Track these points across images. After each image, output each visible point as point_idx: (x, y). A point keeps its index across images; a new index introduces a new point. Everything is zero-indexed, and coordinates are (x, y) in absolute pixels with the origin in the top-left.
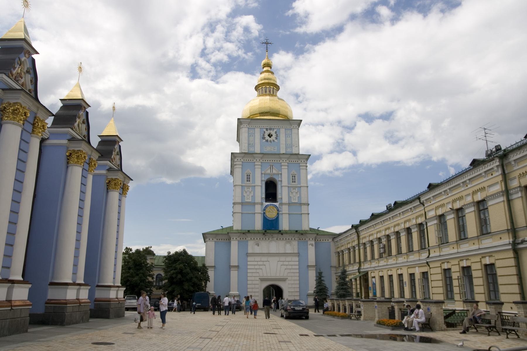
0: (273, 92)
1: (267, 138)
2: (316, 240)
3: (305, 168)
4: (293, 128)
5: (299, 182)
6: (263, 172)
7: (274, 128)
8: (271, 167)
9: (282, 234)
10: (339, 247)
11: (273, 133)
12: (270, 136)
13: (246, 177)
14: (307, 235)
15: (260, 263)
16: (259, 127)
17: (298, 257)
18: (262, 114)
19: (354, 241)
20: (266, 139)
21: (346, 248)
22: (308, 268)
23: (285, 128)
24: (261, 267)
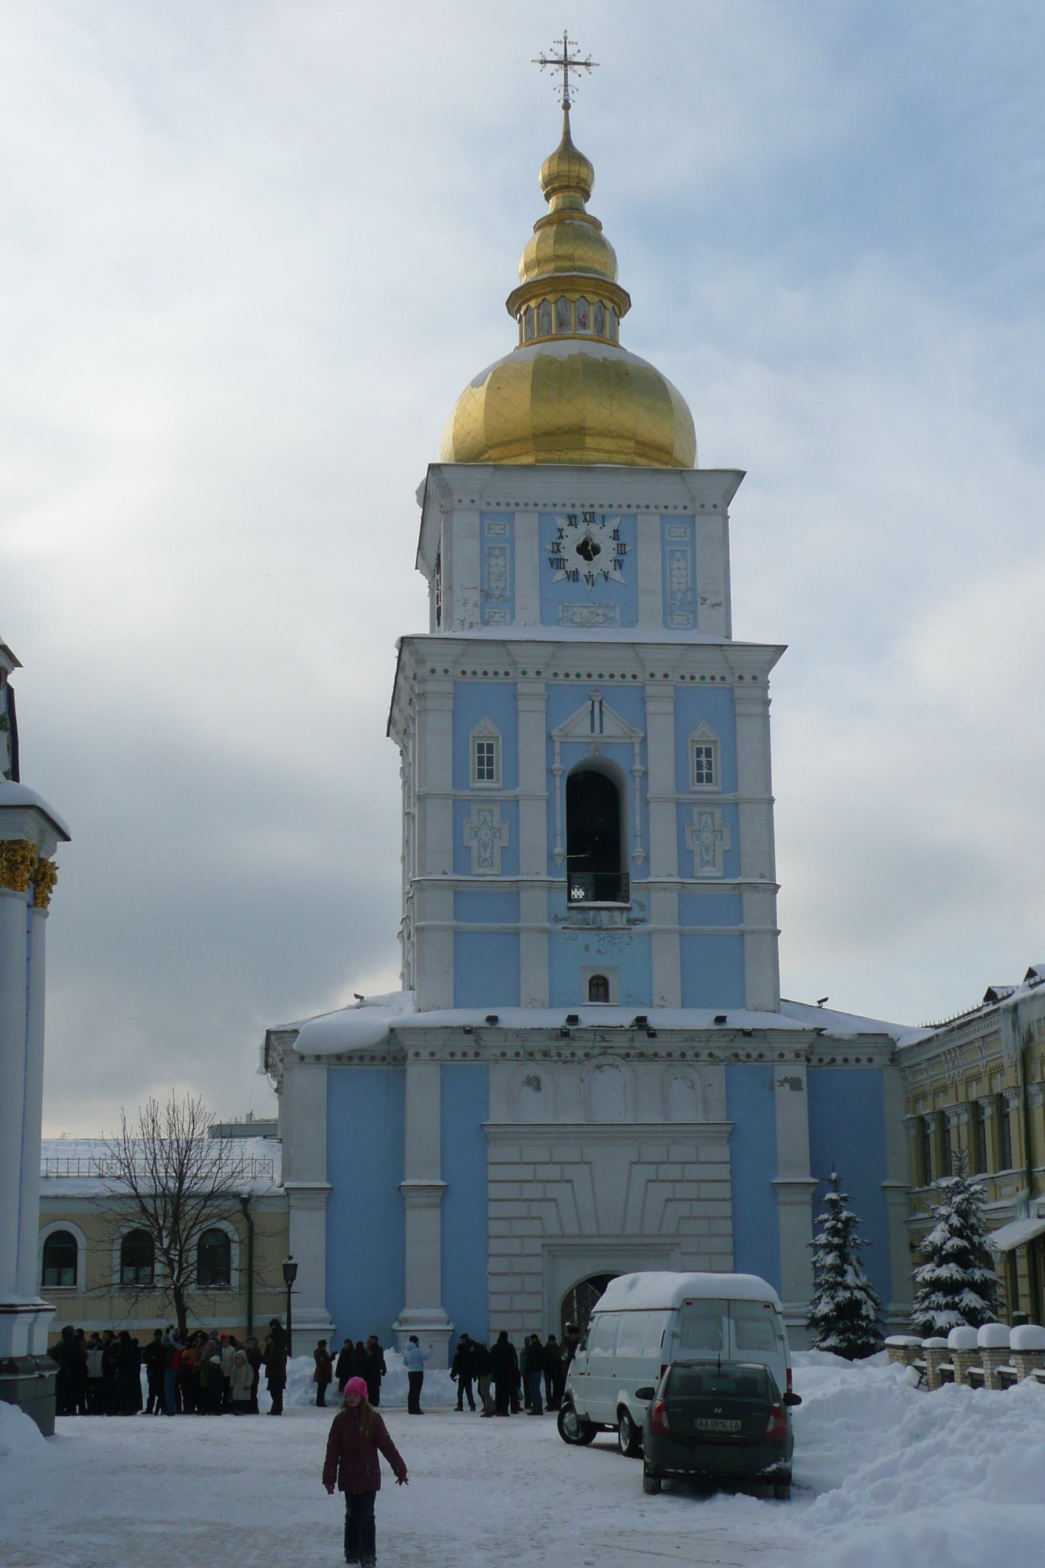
0: (600, 327)
1: (575, 561)
2: (814, 1058)
3: (757, 709)
7: (606, 510)
10: (923, 1097)
11: (601, 536)
12: (587, 550)
13: (473, 756)
15: (544, 1172)
16: (531, 507)
19: (1000, 1070)
20: (570, 566)
21: (962, 1098)
23: (662, 510)
24: (552, 1191)
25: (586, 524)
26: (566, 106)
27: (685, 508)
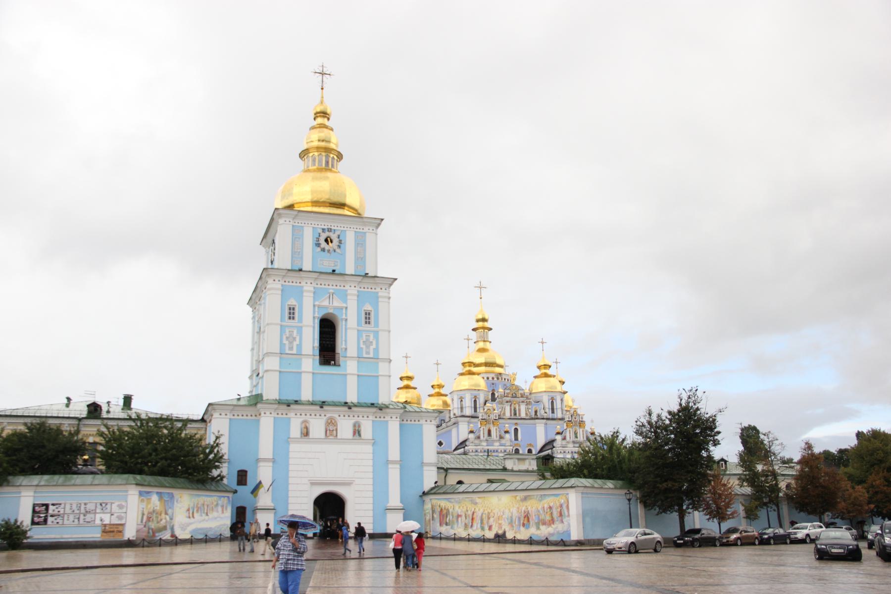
1: (324, 244)
3: (387, 300)
4: (369, 231)
5: (377, 325)
6: (317, 303)
7: (335, 228)
8: (331, 296)
9: (350, 408)
11: (334, 236)
13: (287, 311)
14: (388, 410)
16: (310, 225)
17: (373, 445)
18: (316, 203)
22: (388, 464)
23: (355, 230)
25: (328, 232)
26: (322, 89)
27: (363, 229)
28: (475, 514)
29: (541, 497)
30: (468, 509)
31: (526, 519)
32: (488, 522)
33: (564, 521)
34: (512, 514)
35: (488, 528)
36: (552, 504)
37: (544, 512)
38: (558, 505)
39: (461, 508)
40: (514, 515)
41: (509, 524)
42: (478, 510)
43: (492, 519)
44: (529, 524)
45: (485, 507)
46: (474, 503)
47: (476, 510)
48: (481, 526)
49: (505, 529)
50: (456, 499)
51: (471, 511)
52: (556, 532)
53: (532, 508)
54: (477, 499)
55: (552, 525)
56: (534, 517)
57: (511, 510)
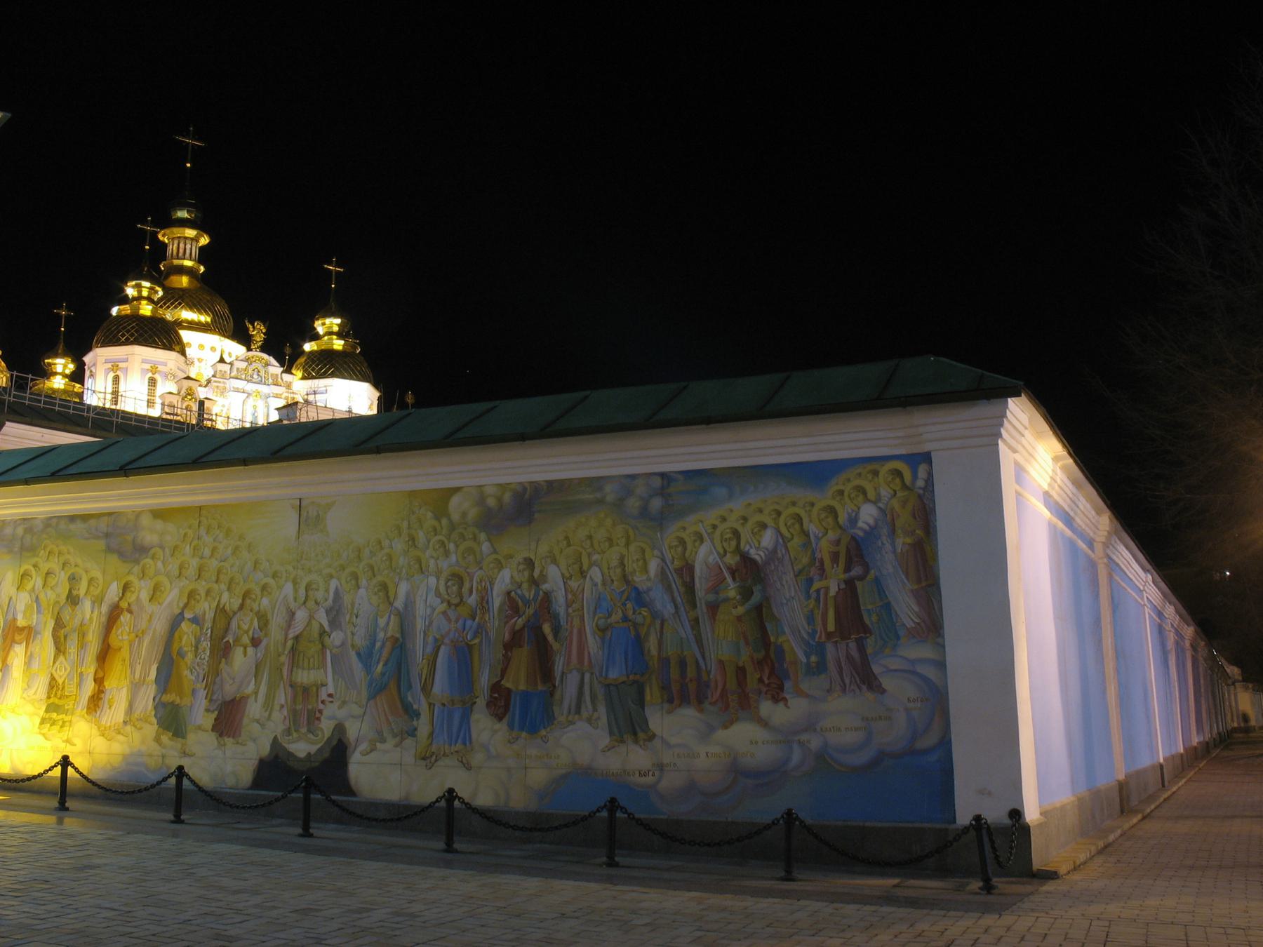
28: (125, 618)
29: (662, 492)
30: (82, 589)
31: (522, 656)
32: (212, 677)
33: (876, 669)
34: (405, 618)
35: (208, 720)
36: (768, 538)
37: (693, 605)
38: (824, 548)
39: (38, 581)
40: (419, 625)
41: (377, 690)
42: (144, 596)
43: (241, 660)
44: (552, 695)
45: (200, 571)
46: (122, 555)
47: (131, 597)
48: (159, 706)
49: (340, 729)
50: (8, 531)
51: (97, 601)
52: (796, 757)
53: (583, 574)
54: (146, 521)
55: (766, 707)
56: (592, 643)
57: (403, 588)
